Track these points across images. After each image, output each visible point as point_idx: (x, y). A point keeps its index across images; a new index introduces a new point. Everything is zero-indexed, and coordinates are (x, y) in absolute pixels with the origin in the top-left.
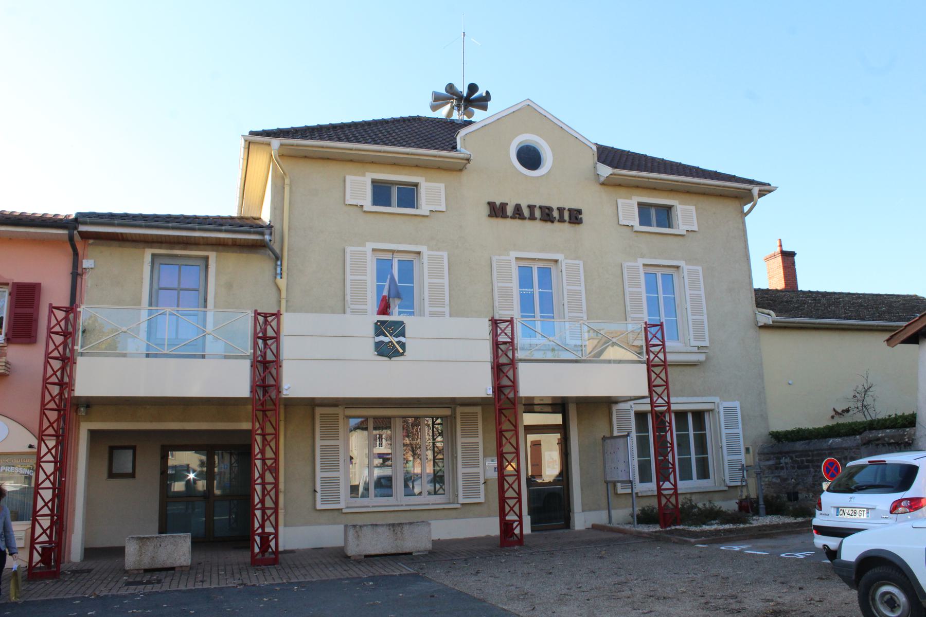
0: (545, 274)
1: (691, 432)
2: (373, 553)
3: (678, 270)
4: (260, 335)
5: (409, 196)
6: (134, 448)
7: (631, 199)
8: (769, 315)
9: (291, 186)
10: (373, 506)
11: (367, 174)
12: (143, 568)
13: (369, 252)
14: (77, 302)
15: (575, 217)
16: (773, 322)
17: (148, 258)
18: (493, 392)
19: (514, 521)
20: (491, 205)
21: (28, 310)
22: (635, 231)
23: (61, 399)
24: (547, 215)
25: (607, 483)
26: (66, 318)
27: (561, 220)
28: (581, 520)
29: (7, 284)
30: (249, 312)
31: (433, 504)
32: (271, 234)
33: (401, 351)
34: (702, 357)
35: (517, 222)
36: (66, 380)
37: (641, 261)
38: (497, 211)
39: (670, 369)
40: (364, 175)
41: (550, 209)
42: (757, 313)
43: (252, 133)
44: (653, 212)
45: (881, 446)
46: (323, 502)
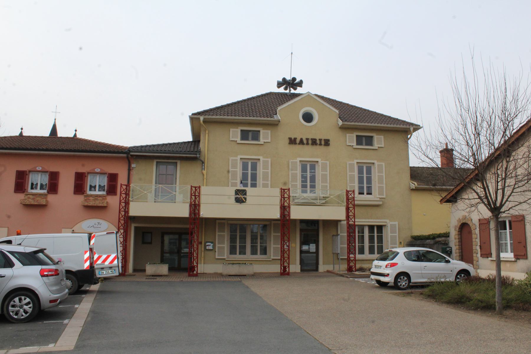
0: (313, 167)
1: (376, 234)
2: (232, 274)
3: (374, 165)
4: (193, 194)
5: (256, 136)
6: (151, 233)
7: (353, 134)
8: (414, 184)
9: (208, 134)
10: (238, 258)
11: (239, 127)
12: (152, 274)
13: (239, 160)
14: (130, 182)
15: (327, 143)
16: (415, 188)
17: (155, 163)
18: (280, 217)
19: (286, 266)
20: (290, 139)
21: (114, 183)
22: (354, 148)
23: (125, 216)
24: (314, 142)
25: (333, 253)
26: (126, 189)
27: (320, 144)
28: (322, 268)
29: (106, 173)
30: (189, 186)
31: (261, 259)
32: (199, 154)
33: (245, 201)
34: (381, 203)
35: (301, 146)
36: (127, 210)
37: (356, 161)
38: (292, 141)
39: (357, 209)
40: (237, 128)
41: (316, 140)
42: (411, 183)
43: (193, 114)
44: (364, 139)
45: (440, 244)
46: (218, 256)
